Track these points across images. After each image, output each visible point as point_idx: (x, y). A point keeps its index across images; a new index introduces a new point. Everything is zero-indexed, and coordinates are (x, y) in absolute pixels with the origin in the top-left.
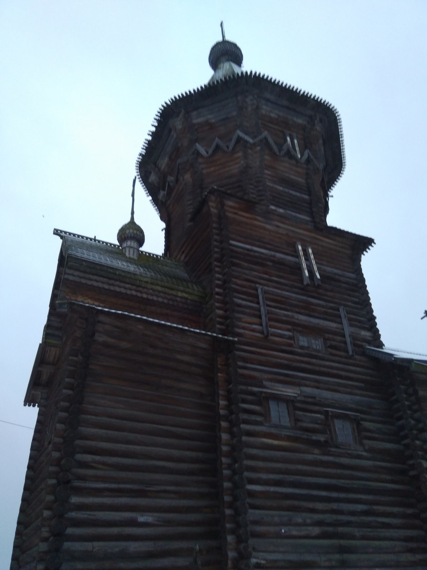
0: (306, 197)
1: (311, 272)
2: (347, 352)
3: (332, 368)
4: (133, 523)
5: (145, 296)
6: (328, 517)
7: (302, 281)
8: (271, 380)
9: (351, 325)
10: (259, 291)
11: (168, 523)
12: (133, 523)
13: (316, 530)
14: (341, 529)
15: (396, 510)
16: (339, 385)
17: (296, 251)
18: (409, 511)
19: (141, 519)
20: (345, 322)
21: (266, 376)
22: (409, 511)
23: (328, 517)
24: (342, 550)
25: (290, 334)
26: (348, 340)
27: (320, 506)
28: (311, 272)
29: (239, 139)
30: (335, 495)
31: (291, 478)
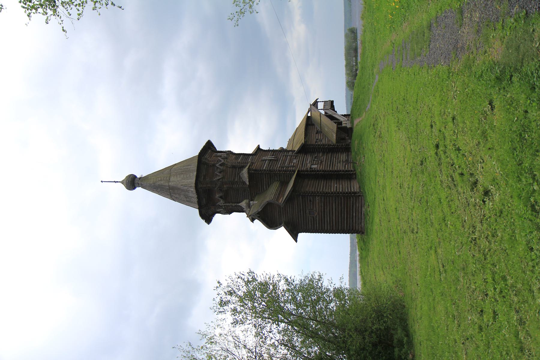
3: (301, 159)
4: (337, 187)
6: (336, 163)
7: (275, 160)
8: (306, 167)
9: (288, 154)
12: (337, 187)
13: (339, 164)
14: (339, 161)
16: (306, 159)
17: (264, 160)
19: (336, 186)
21: (305, 167)
23: (336, 163)
24: (343, 161)
27: (334, 163)
29: (220, 165)
30: (332, 161)
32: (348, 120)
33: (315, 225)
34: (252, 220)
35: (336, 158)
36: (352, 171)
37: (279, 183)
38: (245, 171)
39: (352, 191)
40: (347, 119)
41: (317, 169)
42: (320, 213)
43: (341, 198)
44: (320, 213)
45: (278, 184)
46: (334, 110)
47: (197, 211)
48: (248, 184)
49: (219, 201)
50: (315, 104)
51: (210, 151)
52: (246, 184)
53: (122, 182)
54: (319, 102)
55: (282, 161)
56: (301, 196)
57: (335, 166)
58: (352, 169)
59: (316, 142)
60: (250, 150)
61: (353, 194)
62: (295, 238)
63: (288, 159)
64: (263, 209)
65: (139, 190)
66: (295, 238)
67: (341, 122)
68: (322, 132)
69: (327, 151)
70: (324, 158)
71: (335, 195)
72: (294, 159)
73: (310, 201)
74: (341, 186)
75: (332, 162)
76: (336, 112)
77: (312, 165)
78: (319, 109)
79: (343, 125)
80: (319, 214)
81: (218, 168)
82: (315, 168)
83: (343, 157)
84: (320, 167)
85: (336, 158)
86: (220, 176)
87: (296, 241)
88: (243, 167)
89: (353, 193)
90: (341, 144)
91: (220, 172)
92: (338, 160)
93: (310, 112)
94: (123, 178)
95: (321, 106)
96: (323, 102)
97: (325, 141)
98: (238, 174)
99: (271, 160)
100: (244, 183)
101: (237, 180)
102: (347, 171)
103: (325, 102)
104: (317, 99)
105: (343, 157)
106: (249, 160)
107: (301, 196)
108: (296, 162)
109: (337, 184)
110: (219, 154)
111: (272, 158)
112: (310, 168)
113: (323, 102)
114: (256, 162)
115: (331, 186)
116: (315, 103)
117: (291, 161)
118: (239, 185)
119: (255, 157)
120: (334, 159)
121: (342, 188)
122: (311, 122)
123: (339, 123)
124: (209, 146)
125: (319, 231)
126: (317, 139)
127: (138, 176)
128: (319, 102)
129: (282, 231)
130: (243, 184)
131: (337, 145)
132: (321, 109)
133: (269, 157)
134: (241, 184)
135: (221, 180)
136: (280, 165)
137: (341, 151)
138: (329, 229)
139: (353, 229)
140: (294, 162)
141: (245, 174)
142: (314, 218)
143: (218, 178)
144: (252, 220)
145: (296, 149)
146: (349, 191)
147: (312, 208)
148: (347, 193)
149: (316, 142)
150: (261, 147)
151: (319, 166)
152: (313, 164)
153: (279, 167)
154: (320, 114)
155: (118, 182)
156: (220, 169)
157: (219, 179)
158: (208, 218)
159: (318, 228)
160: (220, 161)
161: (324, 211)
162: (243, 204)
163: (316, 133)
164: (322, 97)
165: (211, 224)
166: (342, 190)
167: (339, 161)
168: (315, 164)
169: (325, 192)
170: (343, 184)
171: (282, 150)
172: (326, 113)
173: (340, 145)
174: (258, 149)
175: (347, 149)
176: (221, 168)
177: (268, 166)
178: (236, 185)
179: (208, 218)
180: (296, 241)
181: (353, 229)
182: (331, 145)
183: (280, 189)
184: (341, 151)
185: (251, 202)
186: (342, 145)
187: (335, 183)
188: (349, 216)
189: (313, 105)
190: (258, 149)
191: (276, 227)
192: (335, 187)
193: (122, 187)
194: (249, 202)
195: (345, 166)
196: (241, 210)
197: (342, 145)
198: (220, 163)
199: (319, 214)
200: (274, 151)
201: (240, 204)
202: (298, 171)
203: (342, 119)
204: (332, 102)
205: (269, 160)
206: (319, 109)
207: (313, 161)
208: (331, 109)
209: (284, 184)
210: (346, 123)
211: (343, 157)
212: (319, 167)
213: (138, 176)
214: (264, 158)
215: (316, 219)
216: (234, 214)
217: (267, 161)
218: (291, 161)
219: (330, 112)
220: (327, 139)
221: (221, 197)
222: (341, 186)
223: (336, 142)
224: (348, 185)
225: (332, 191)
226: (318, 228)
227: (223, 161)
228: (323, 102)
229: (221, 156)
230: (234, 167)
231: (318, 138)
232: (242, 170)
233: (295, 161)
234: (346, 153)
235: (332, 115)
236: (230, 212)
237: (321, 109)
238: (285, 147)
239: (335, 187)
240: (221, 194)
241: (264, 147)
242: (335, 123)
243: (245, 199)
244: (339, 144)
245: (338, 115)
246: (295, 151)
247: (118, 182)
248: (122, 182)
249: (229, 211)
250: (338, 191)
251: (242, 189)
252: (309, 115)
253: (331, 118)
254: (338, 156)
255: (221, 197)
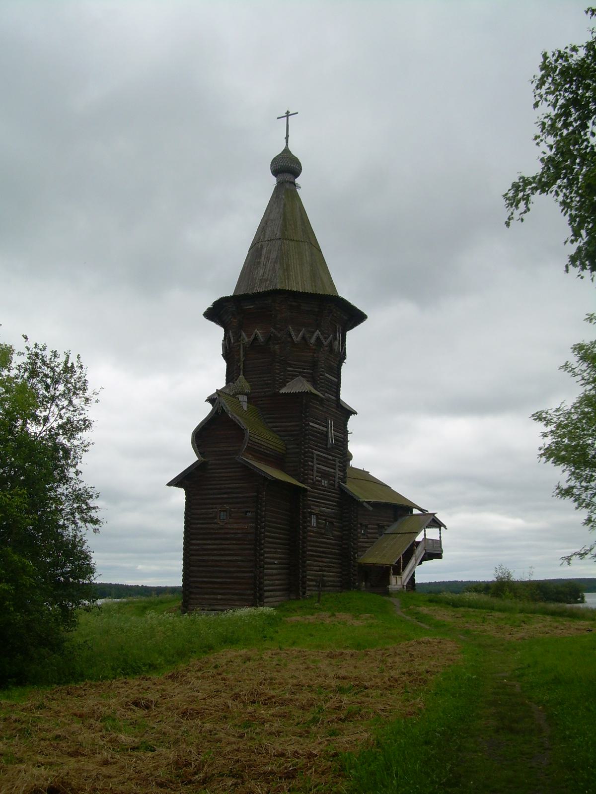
0: (336, 380)
1: (332, 440)
2: (334, 486)
5: (268, 452)
6: (321, 564)
7: (326, 445)
8: (314, 505)
10: (315, 456)
11: (280, 564)
14: (324, 568)
15: (336, 561)
16: (329, 505)
18: (340, 561)
19: (275, 562)
20: (338, 468)
22: (340, 561)
23: (321, 564)
24: (324, 576)
25: (319, 479)
26: (337, 480)
28: (332, 440)
30: (324, 555)
31: (314, 548)
32: (404, 586)
33: (201, 522)
34: (211, 400)
35: (330, 562)
36: (304, 593)
37: (284, 452)
38: (307, 387)
39: (267, 594)
40: (405, 584)
41: (309, 526)
42: (223, 531)
43: (251, 572)
44: (223, 531)
45: (280, 451)
46: (424, 559)
47: (230, 293)
48: (281, 392)
49: (249, 336)
50: (437, 524)
51: (346, 318)
52: (281, 387)
53: (286, 151)
54: (440, 530)
55: (325, 458)
56: (256, 494)
57: (314, 561)
58: (308, 593)
59: (361, 524)
60: (346, 396)
61: (258, 595)
62: (177, 482)
63: (328, 469)
64: (232, 420)
65: (273, 181)
66: (177, 482)
67: (399, 574)
68: (381, 535)
69: (343, 546)
70: (330, 539)
71: (258, 560)
72: (329, 482)
73: (246, 513)
74: (275, 572)
75: (321, 555)
76: (420, 563)
77: (317, 516)
78: (425, 531)
79: (393, 579)
80: (220, 529)
81: (313, 332)
82: (310, 522)
83: (330, 576)
84: (313, 532)
85: (330, 562)
86: (297, 339)
87: (169, 484)
88: (314, 383)
89: (261, 595)
90: (356, 573)
91: (303, 338)
92: (325, 566)
93: (418, 512)
94: (295, 151)
95: (432, 534)
96: (439, 539)
97: (363, 542)
98: (300, 372)
99: (327, 436)
100: (283, 384)
101: (289, 371)
102: (304, 583)
103: (439, 542)
104: (445, 526)
105: (331, 576)
106: (326, 394)
107: (256, 494)
108: (323, 486)
109: (280, 564)
110: (339, 335)
111: (331, 440)
112: (311, 513)
113: (440, 537)
114: (324, 407)
115: (275, 553)
116: (437, 523)
117: (325, 475)
118: (278, 374)
119: (334, 405)
120: (328, 560)
121: (272, 575)
122: (401, 516)
123: (398, 570)
124: (356, 317)
125: (189, 529)
126: (366, 527)
127: (297, 181)
128: (440, 530)
129: (191, 458)
130: (280, 383)
131: (354, 566)
132: (425, 535)
133: (332, 432)
134: (281, 379)
135: (289, 339)
136: (318, 455)
137: (344, 573)
138: (191, 547)
139: (191, 593)
140: (323, 481)
141: (299, 386)
142: (215, 518)
143: (293, 333)
144: (211, 400)
145: (350, 487)
146: (266, 588)
147: (232, 515)
148: (261, 583)
149: (361, 524)
150: (352, 417)
151: (315, 530)
152: (317, 518)
153: (313, 453)
154: (417, 533)
155: (287, 142)
156: (310, 338)
157: (290, 335)
158: (216, 313)
159: (194, 526)
160: (326, 338)
161: (227, 539)
162: (242, 381)
163: (378, 525)
164: (447, 539)
165: (204, 319)
166: (266, 575)
167: (324, 568)
168: (318, 523)
169: (263, 542)
170: (279, 577)
171: (348, 457)
172: (418, 543)
173: (355, 570)
174: (349, 412)
175: (346, 585)
176: (313, 340)
177: (316, 432)
178: (278, 369)
179: (216, 313)
180: (169, 484)
181: (191, 593)
182: (355, 553)
183: (271, 453)
184: (344, 573)
185: (245, 398)
186: (355, 575)
187: (280, 561)
188: (216, 586)
189: (433, 519)
190: (349, 412)
191: (198, 446)
192: (272, 561)
193: (278, 150)
194: (246, 394)
195: (312, 580)
196: (231, 376)
197: (355, 575)
198: (321, 337)
199: (220, 529)
200: (345, 442)
201: (241, 376)
202: (306, 490)
203: (406, 575)
204: (439, 556)
205: (327, 432)
206: (425, 531)
207: (324, 518)
208: (425, 554)
209: (278, 462)
210: (396, 583)
211: (330, 576)
212: (312, 529)
213: (297, 181)
214: (331, 423)
215: (211, 523)
216: (223, 364)
217: (325, 429)
218: (325, 475)
219: (419, 552)
220: (367, 545)
221: (256, 338)
222: (275, 572)
223: (360, 564)
224: (277, 586)
225: (266, 555)
226: (194, 526)
227: (325, 343)
228: (440, 537)
229: (335, 338)
230: (314, 364)
231: (370, 529)
232: (308, 381)
233: (325, 483)
234: (340, 582)
235: (414, 555)
236: (227, 355)
237: (425, 535)
238: (351, 463)
239: (272, 561)
240: (261, 339)
241: (352, 423)
242: (399, 562)
243: (251, 386)
244: (356, 569)
245: (414, 567)
246: (345, 482)
247: (287, 142)
248: (286, 151)
249: (229, 353)
250: (266, 566)
251: (270, 380)
252: (415, 511)
253: (408, 555)
254: (333, 567)
255: (256, 338)
